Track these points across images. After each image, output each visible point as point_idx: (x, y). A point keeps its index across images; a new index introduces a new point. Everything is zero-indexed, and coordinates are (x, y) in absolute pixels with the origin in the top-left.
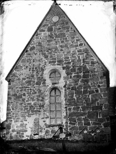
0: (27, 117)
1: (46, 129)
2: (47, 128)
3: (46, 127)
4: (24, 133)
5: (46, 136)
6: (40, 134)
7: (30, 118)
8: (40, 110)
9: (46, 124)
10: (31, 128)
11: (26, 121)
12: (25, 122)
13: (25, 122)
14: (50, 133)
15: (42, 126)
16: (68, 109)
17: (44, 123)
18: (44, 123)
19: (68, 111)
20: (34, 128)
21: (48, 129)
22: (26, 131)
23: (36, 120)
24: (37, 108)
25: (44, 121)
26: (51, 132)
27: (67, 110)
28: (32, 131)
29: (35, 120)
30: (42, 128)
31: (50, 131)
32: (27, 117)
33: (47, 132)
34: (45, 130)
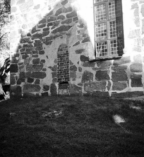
0: (44, 45)
1: (85, 69)
2: (85, 68)
3: (85, 65)
4: (41, 80)
5: (85, 86)
6: (71, 82)
7: (51, 46)
8: (70, 25)
9: (84, 58)
10: (53, 70)
11: (42, 53)
12: (41, 57)
13: (41, 57)
14: (94, 78)
15: (75, 63)
16: (140, 10)
17: (79, 55)
18: (79, 55)
19: (140, 14)
20: (58, 68)
21: (89, 69)
22: (44, 75)
23: (61, 50)
24: (64, 20)
25: (79, 52)
26: (96, 75)
27: (136, 14)
28: (54, 75)
29: (59, 51)
30: (74, 68)
31: (94, 73)
32: (44, 45)
33: (86, 77)
34: (82, 72)
